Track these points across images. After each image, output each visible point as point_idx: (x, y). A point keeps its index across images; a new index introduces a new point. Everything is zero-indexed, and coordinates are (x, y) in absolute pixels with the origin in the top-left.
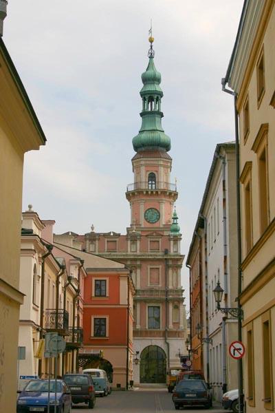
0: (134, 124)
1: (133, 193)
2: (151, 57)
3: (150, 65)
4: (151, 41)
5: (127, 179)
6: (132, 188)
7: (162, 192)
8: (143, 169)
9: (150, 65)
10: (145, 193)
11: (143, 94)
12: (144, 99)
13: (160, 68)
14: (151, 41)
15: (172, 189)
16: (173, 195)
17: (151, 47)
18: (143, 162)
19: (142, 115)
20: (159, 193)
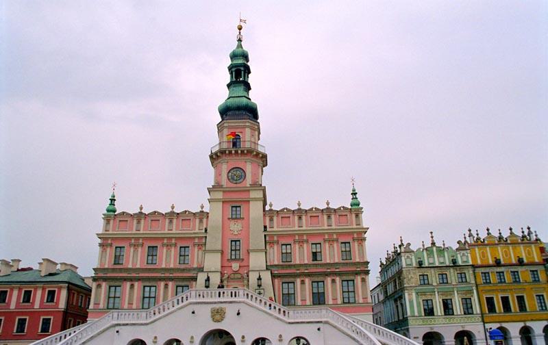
0: (222, 95)
1: (216, 154)
2: (240, 40)
3: (240, 46)
4: (240, 28)
5: (212, 140)
6: (217, 149)
7: (247, 150)
8: (226, 132)
9: (240, 46)
10: (227, 152)
11: (230, 68)
12: (231, 73)
13: (246, 47)
14: (240, 28)
15: (260, 149)
16: (263, 159)
17: (240, 33)
18: (225, 125)
19: (229, 86)
20: (245, 152)
